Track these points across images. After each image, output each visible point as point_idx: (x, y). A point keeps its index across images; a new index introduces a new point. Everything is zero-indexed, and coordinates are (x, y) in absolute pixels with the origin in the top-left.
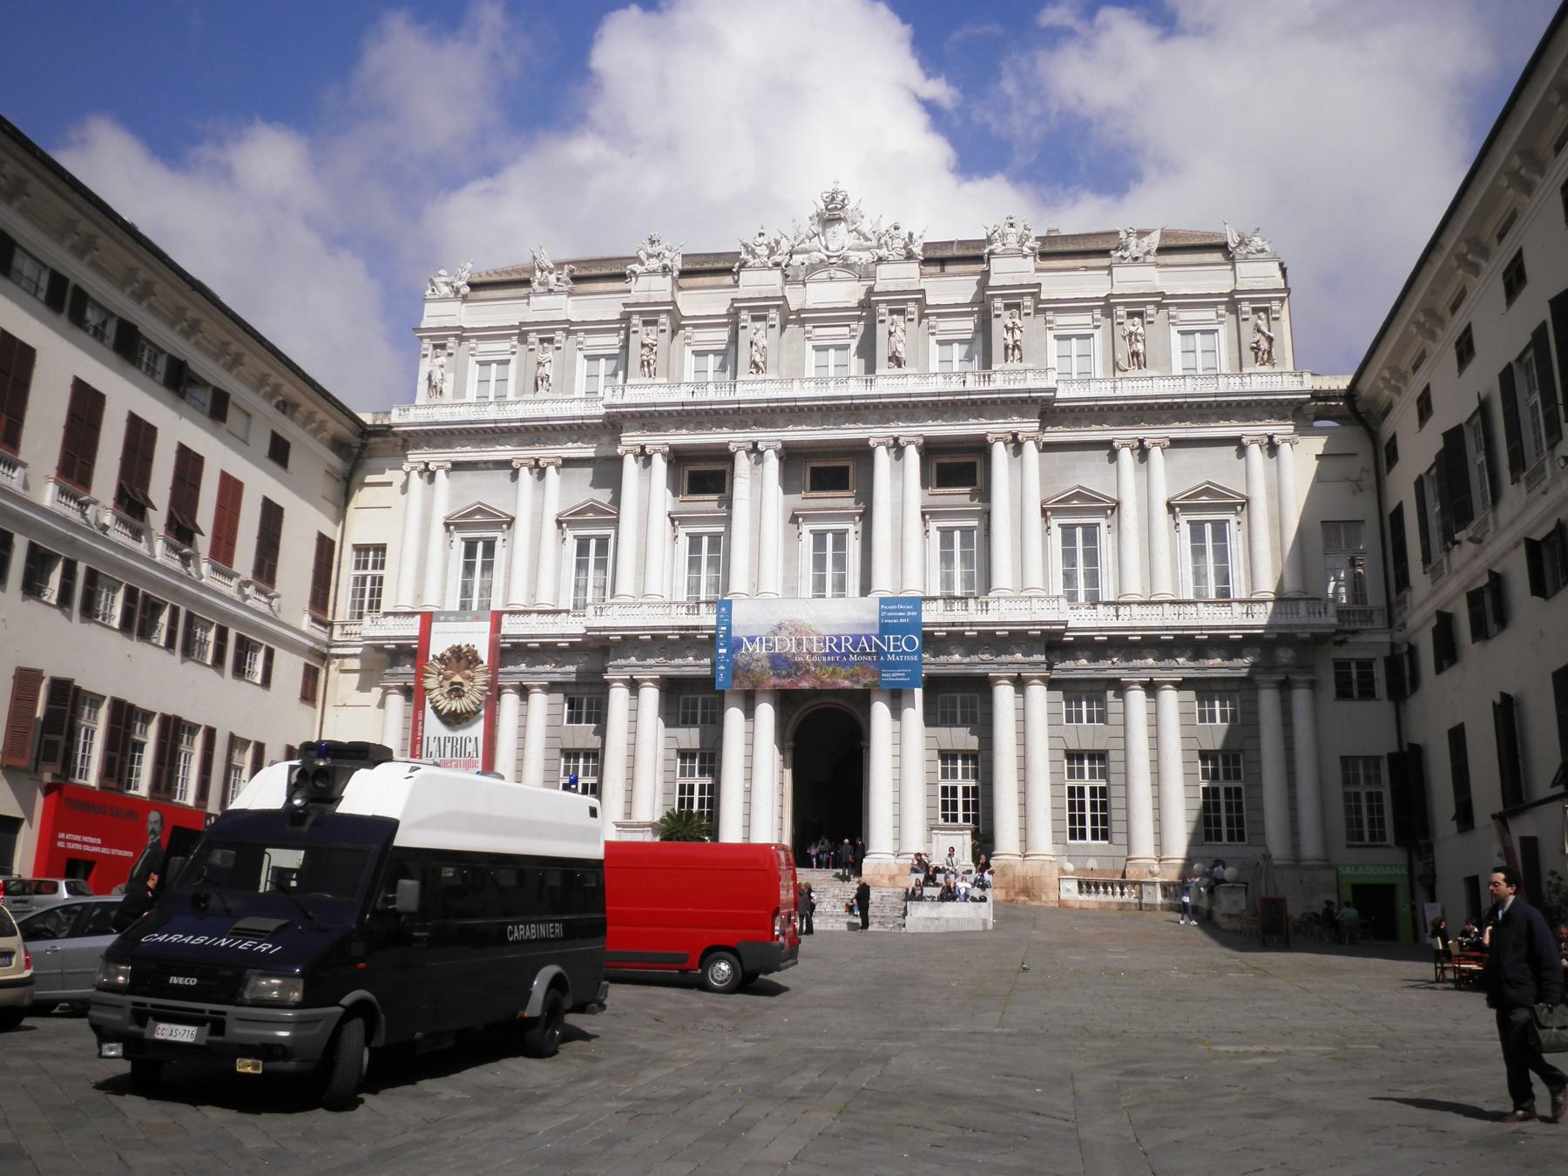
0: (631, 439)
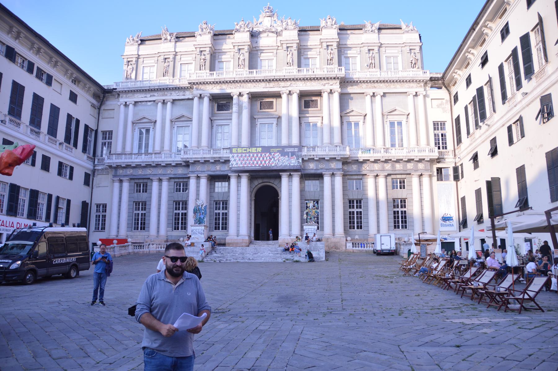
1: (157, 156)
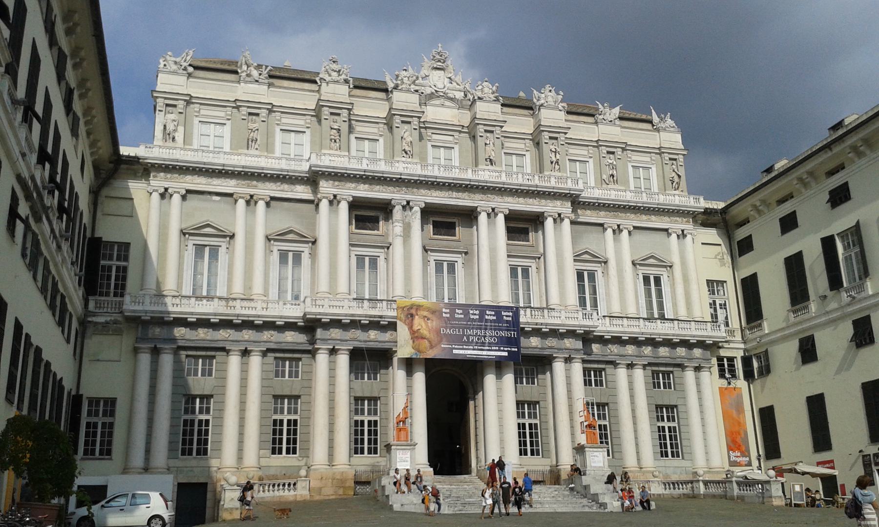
0: (326, 188)
1: (245, 304)
